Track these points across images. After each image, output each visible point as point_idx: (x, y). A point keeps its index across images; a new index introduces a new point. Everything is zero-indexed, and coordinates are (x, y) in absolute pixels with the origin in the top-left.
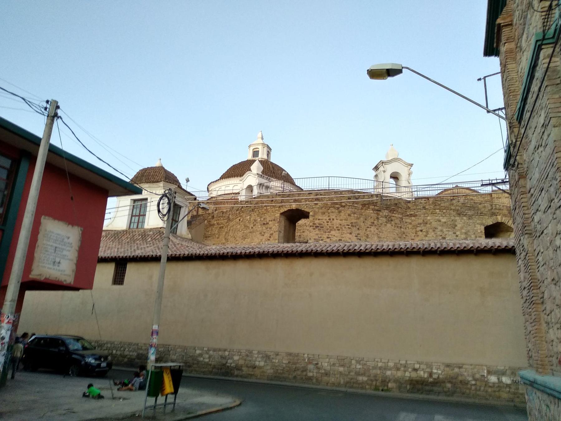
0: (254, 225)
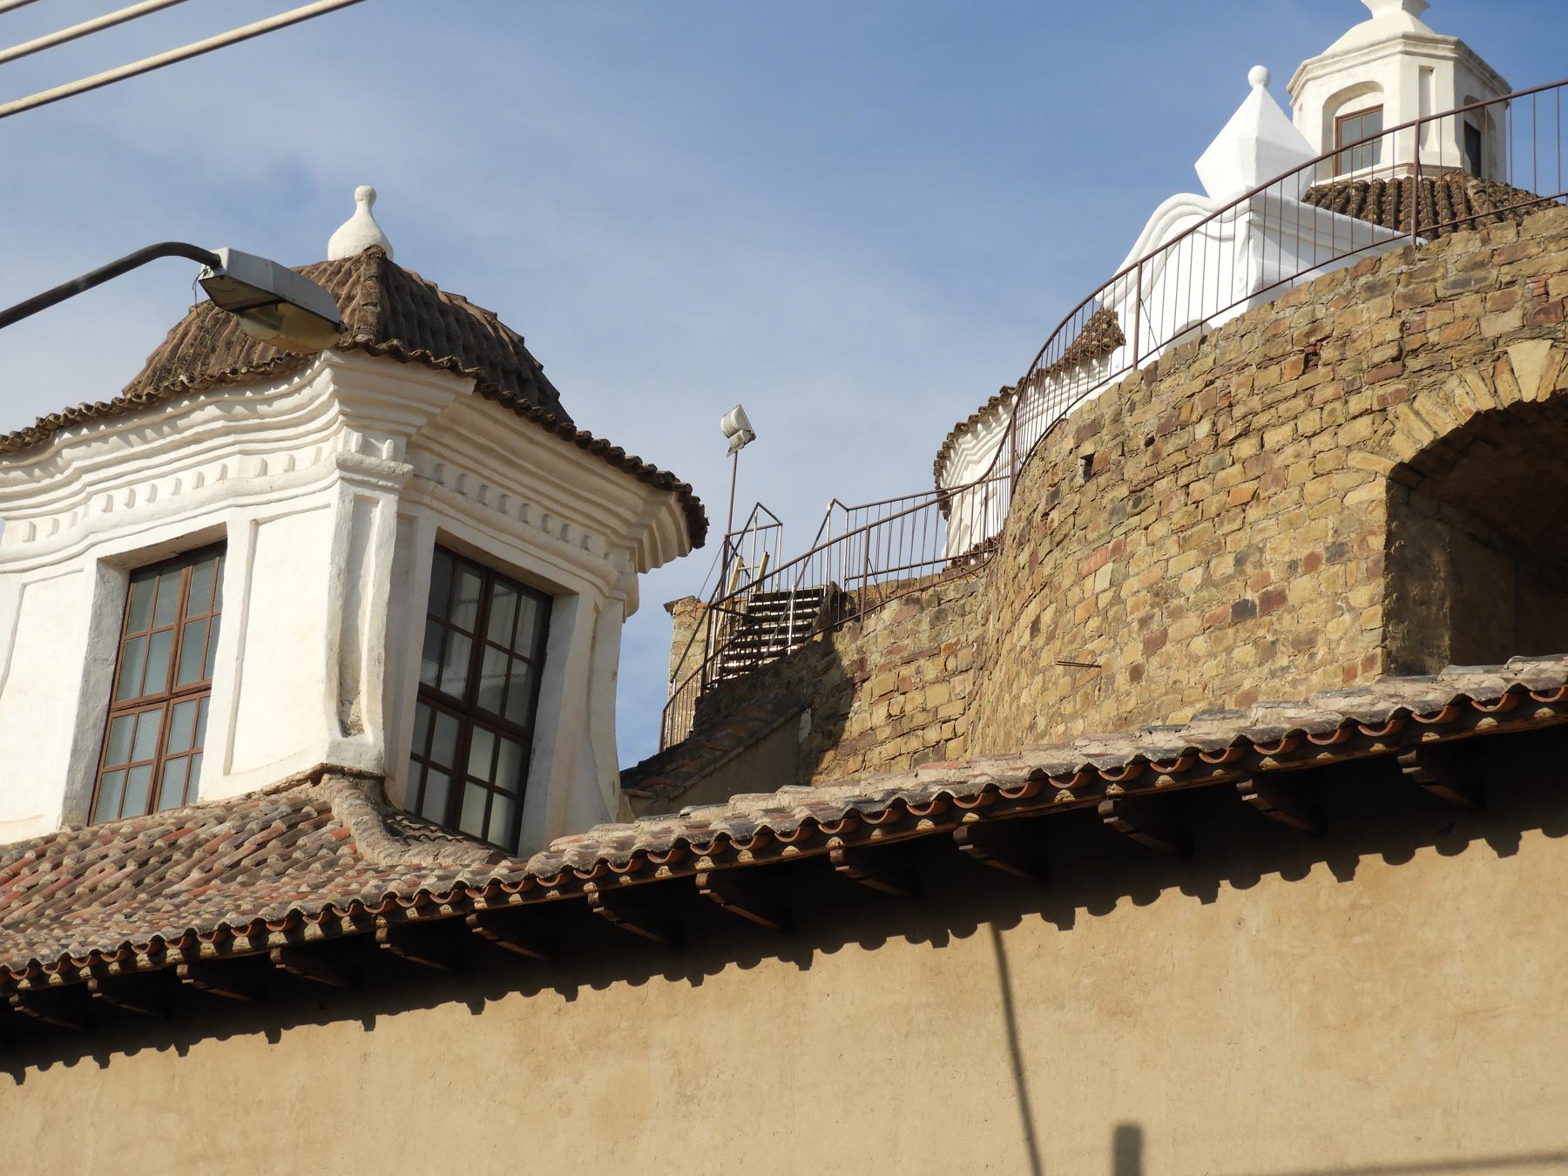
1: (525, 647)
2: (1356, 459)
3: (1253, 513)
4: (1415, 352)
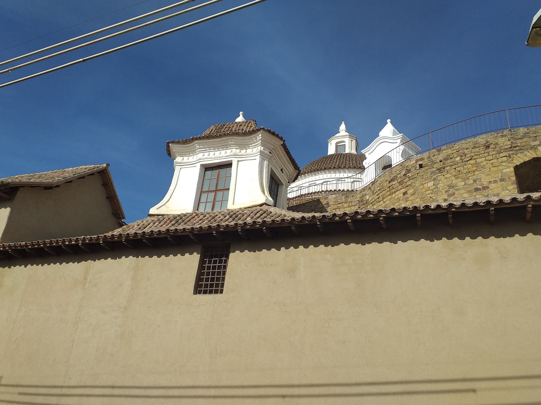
0: (450, 196)
1: (275, 192)
2: (504, 164)
3: (476, 173)
4: (515, 147)
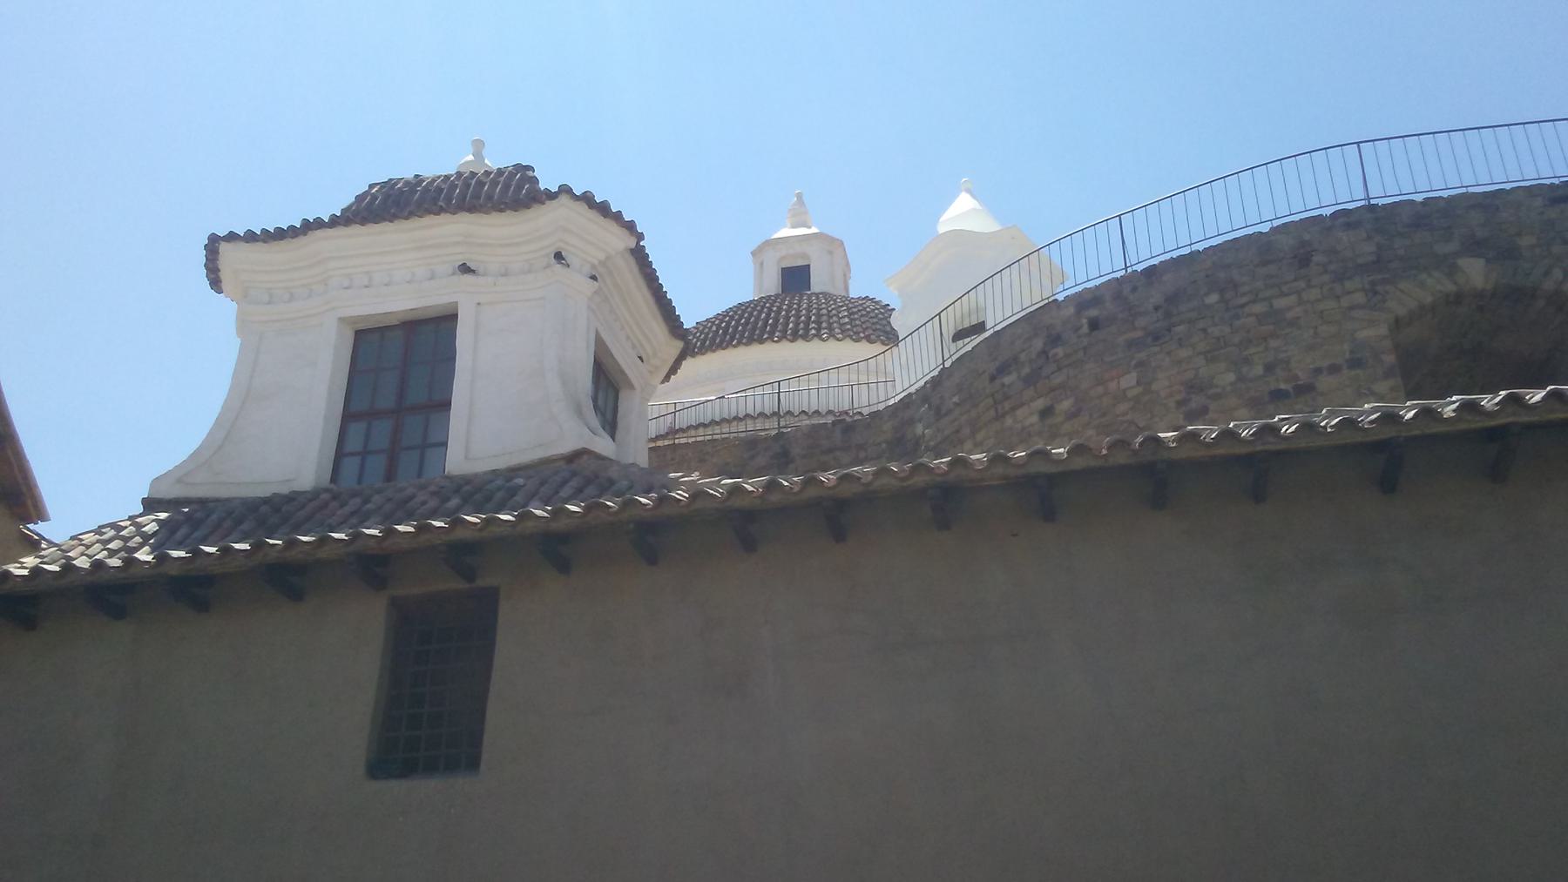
1: (609, 416)
